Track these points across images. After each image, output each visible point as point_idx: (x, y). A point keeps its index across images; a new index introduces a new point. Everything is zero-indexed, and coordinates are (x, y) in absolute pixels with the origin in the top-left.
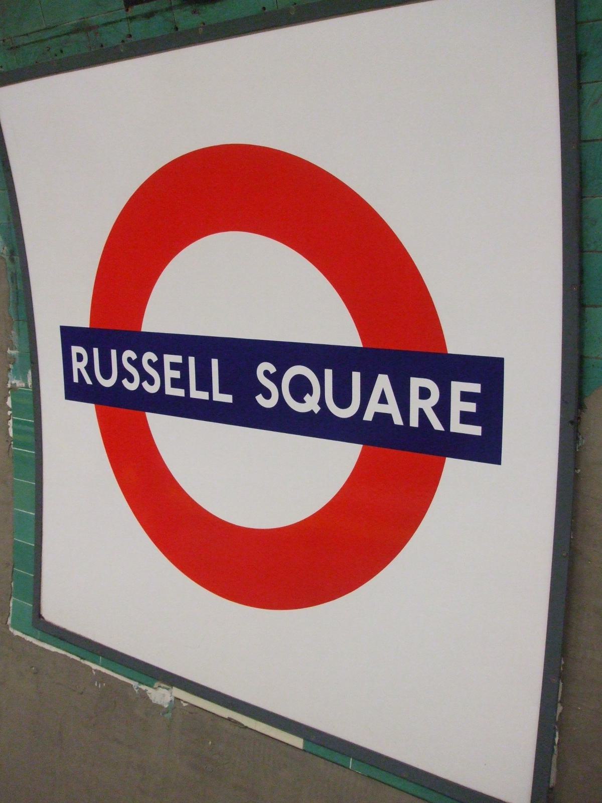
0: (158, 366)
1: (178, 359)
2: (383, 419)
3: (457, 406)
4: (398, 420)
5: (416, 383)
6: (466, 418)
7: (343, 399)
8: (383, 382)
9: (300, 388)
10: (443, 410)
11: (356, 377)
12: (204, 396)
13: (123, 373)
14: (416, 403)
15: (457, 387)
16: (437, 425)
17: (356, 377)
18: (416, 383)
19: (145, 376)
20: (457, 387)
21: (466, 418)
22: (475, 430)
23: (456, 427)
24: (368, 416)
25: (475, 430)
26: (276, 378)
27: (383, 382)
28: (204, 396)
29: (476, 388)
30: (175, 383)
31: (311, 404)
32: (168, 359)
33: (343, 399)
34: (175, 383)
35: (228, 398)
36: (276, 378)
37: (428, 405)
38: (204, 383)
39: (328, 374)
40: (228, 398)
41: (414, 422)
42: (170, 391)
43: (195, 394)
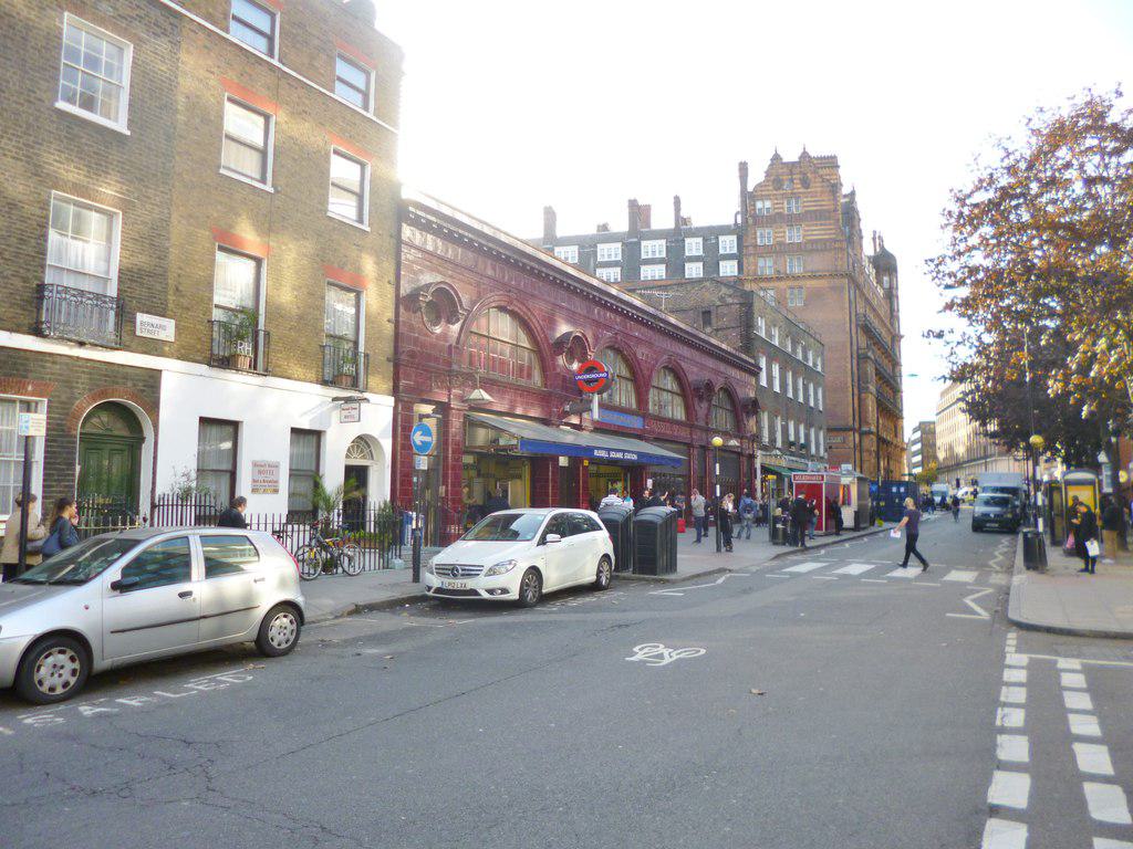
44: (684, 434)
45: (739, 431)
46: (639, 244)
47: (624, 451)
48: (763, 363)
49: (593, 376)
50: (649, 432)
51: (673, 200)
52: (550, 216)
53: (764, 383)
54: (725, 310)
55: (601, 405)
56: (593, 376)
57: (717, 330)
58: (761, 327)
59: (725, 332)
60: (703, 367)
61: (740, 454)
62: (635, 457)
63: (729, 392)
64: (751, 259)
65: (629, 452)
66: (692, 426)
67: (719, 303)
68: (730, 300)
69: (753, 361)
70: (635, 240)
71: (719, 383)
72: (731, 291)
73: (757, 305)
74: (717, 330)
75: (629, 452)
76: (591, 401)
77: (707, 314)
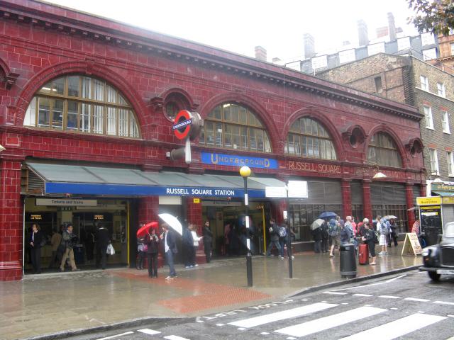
44: (335, 171)
45: (404, 166)
46: (366, 47)
47: (213, 189)
48: (428, 113)
49: (183, 124)
51: (387, 16)
52: (309, 39)
53: (430, 125)
54: (391, 74)
55: (193, 149)
56: (183, 124)
57: (387, 90)
58: (424, 85)
59: (394, 90)
60: (351, 116)
61: (405, 185)
62: (232, 193)
63: (384, 133)
64: (445, 45)
65: (221, 189)
67: (387, 70)
68: (395, 66)
69: (415, 111)
70: (364, 46)
71: (369, 129)
72: (394, 60)
73: (417, 67)
74: (387, 90)
75: (221, 189)
76: (185, 146)
77: (378, 79)
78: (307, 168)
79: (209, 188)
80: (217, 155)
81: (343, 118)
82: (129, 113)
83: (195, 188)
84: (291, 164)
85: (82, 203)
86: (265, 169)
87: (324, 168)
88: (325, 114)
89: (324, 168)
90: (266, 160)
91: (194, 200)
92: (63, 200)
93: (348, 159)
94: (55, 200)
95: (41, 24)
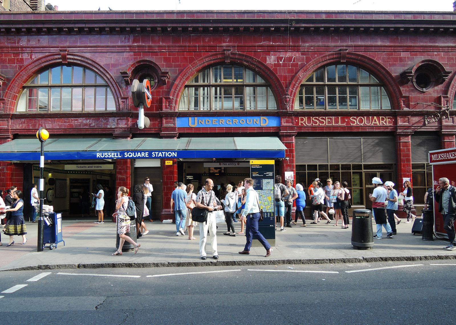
0: (111, 154)
1: (114, 153)
2: (139, 157)
3: (146, 154)
4: (141, 156)
5: (142, 153)
6: (147, 155)
7: (135, 155)
8: (139, 153)
9: (130, 155)
10: (145, 155)
11: (136, 153)
12: (117, 157)
13: (105, 155)
14: (142, 155)
15: (146, 153)
16: (144, 156)
17: (136, 153)
18: (142, 153)
19: (108, 155)
20: (146, 153)
21: (147, 155)
22: (148, 156)
23: (146, 156)
24: (138, 156)
25: (148, 156)
26: (127, 154)
27: (139, 153)
28: (117, 157)
29: (148, 153)
30: (113, 156)
31: (131, 156)
32: (112, 153)
33: (135, 155)
34: (113, 156)
35: (121, 157)
36: (127, 154)
37: (143, 155)
38: (117, 155)
39: (133, 153)
40: (121, 157)
41: (142, 156)
42: (112, 157)
43: (116, 157)
44: (386, 122)
50: (286, 128)
66: (393, 115)
78: (329, 122)
79: (145, 151)
80: (196, 118)
81: (403, 55)
82: (381, 89)
83: (128, 151)
84: (302, 120)
85: (101, 167)
86: (261, 128)
87: (361, 121)
88: (368, 55)
89: (361, 121)
90: (262, 118)
91: (166, 162)
92: (85, 165)
93: (408, 106)
94: (79, 166)
95: (216, 29)
